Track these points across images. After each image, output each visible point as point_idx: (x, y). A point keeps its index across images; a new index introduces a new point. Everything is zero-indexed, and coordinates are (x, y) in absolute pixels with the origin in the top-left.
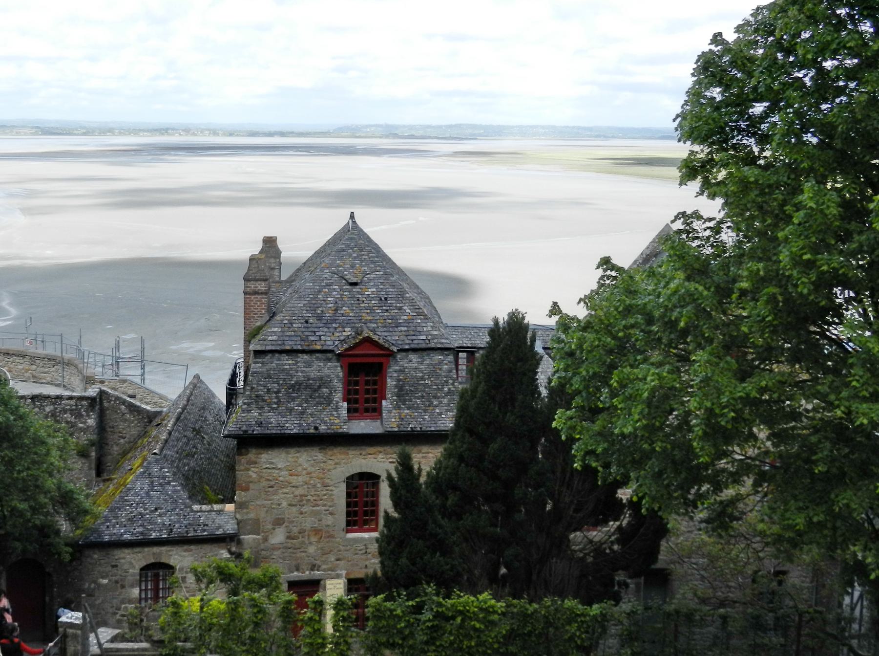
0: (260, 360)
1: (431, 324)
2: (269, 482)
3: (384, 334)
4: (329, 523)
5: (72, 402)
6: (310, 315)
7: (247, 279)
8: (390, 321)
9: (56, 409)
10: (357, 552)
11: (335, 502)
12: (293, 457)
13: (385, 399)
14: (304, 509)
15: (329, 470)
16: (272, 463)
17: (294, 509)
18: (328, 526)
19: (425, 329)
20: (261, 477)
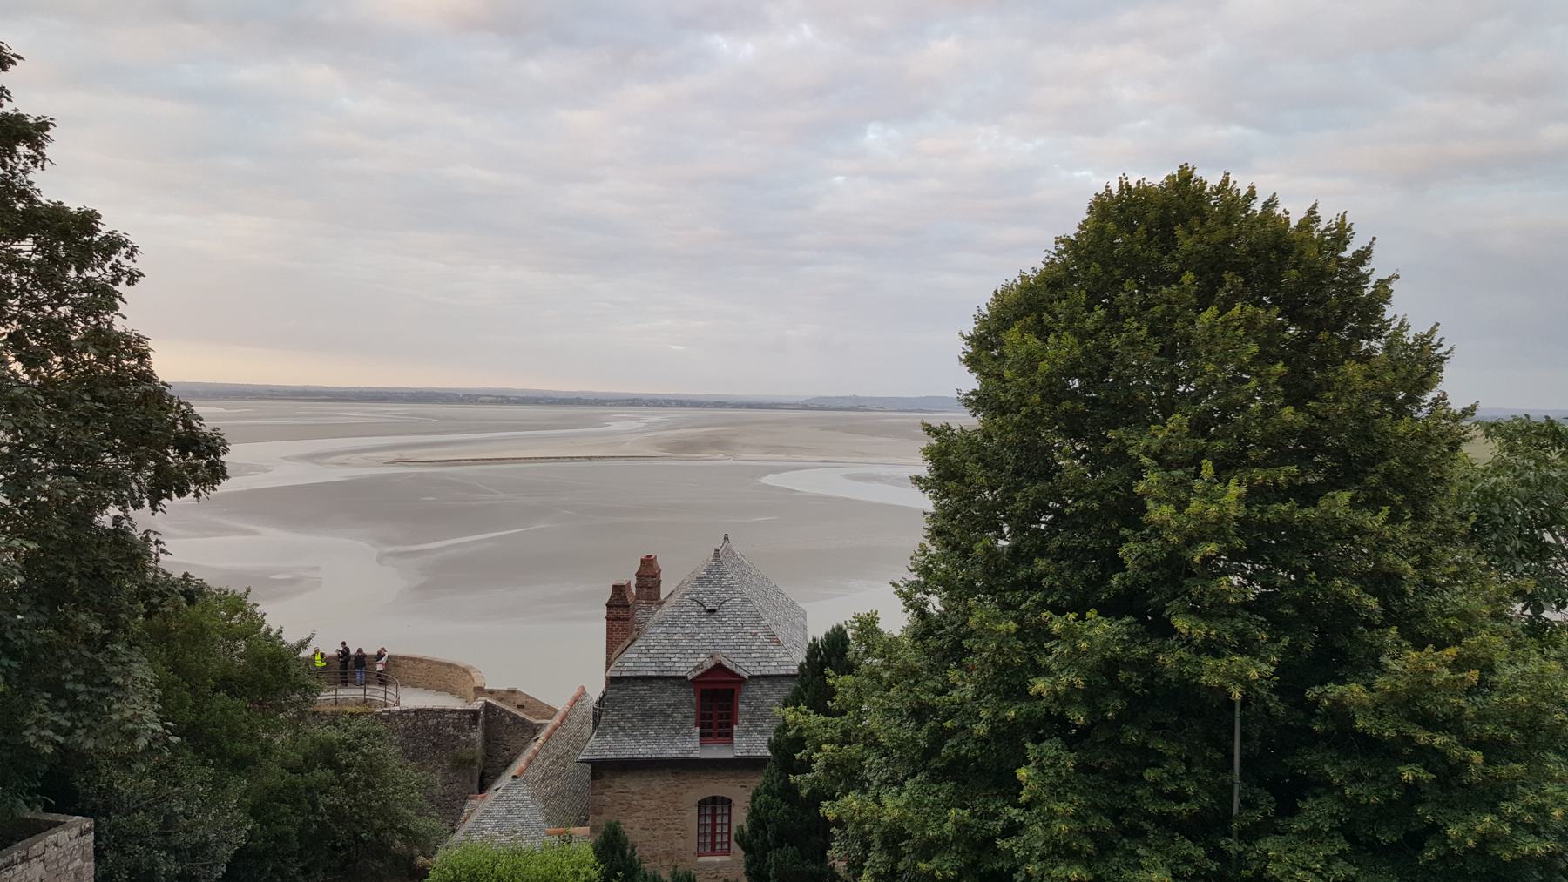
0: (616, 686)
1: (784, 651)
3: (737, 660)
4: (681, 847)
5: (455, 716)
6: (667, 641)
7: (609, 606)
8: (744, 647)
9: (439, 722)
10: (708, 876)
13: (737, 724)
14: (656, 834)
15: (681, 794)
17: (647, 833)
18: (680, 849)
19: (777, 656)
20: (615, 801)
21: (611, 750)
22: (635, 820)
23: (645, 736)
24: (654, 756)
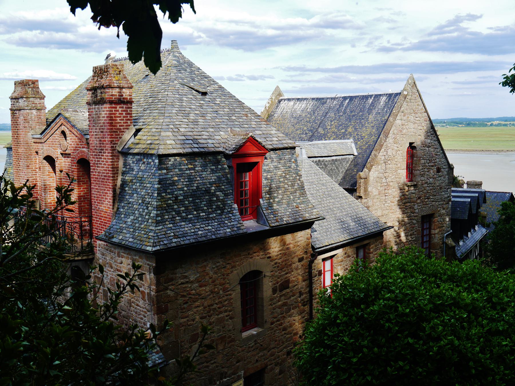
2: (183, 299)
11: (234, 305)
12: (202, 267)
13: (262, 198)
16: (186, 277)
21: (176, 236)
22: (195, 310)
23: (198, 217)
24: (214, 237)
